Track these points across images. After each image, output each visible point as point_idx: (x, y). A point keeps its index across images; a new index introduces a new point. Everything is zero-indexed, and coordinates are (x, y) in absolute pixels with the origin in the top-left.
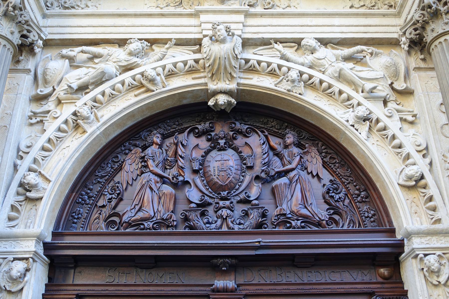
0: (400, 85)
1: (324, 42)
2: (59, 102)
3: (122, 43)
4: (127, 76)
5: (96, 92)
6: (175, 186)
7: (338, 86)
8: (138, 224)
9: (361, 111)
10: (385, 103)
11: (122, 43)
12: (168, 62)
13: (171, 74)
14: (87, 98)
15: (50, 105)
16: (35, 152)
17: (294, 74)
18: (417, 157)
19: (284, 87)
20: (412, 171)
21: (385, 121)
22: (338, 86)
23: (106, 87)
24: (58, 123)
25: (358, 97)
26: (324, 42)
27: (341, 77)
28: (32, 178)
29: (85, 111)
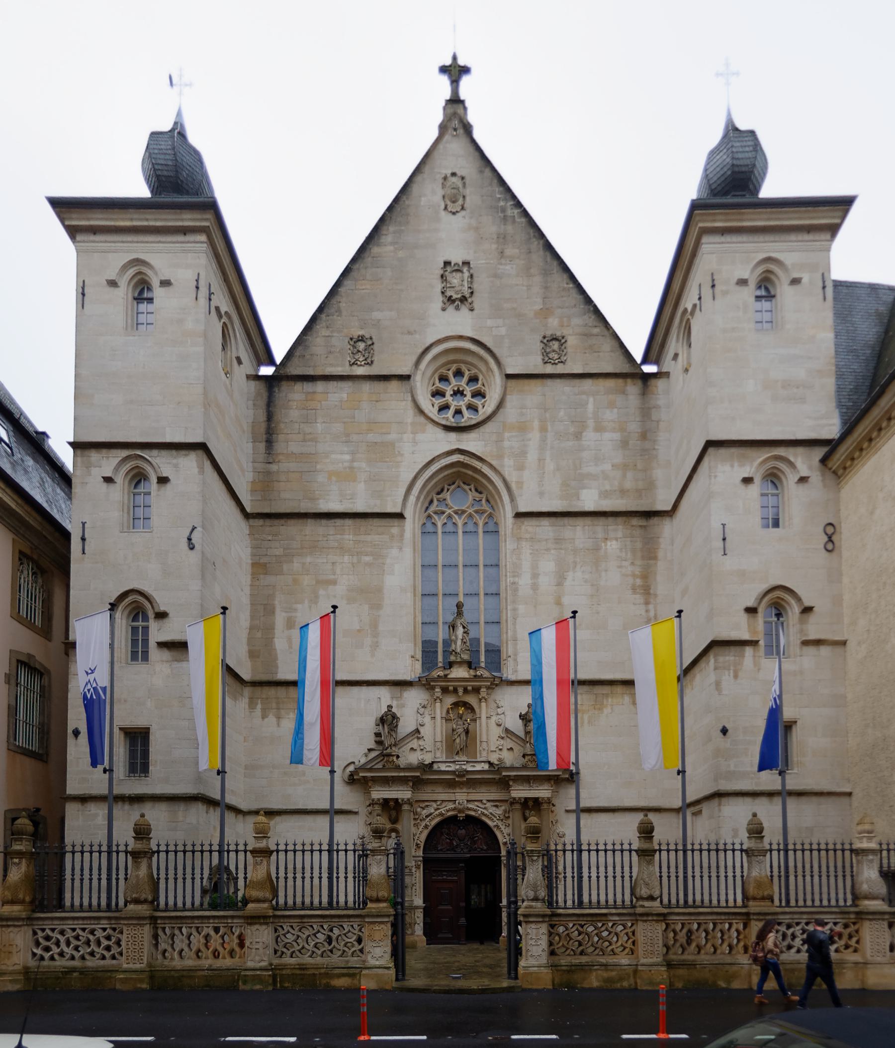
0: (507, 815)
1: (488, 801)
2: (421, 820)
3: (435, 801)
4: (437, 812)
5: (430, 818)
6: (449, 839)
7: (490, 816)
8: (441, 850)
9: (495, 823)
10: (502, 820)
11: (435, 801)
12: (447, 808)
13: (448, 811)
14: (428, 819)
15: (419, 821)
16: (418, 835)
17: (479, 812)
18: (506, 836)
19: (477, 815)
20: (505, 840)
21: (501, 826)
22: (490, 816)
23: (432, 816)
24: (422, 827)
25: (495, 819)
26: (488, 801)
27: (491, 813)
28: (419, 842)
29: (428, 823)
